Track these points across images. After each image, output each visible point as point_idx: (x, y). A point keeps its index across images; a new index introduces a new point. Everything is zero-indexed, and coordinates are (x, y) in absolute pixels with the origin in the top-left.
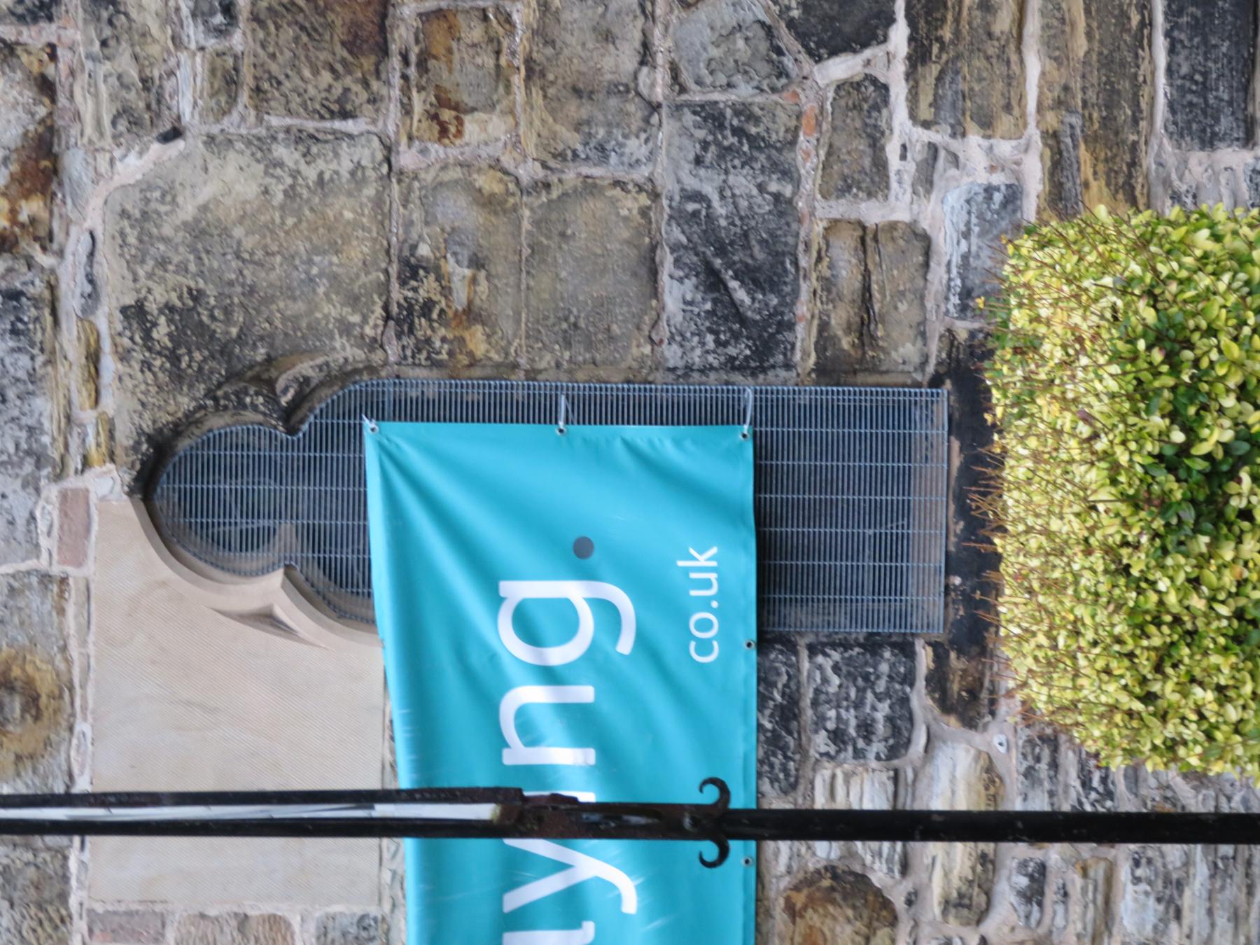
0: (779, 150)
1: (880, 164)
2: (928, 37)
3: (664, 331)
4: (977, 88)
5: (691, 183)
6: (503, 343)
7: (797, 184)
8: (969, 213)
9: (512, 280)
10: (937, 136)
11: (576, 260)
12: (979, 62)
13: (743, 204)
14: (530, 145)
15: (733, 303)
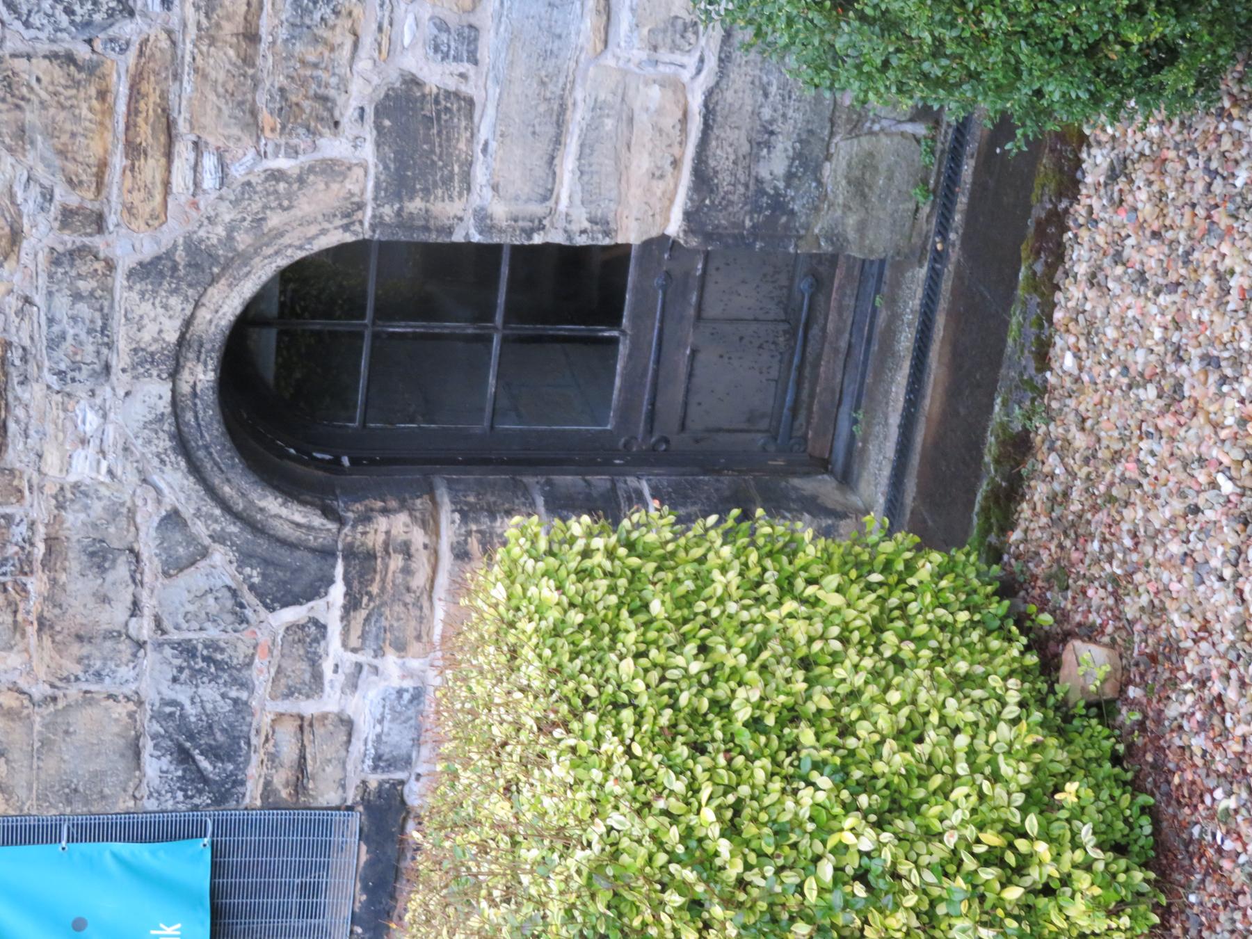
0: (239, 670)
1: (317, 677)
2: (360, 592)
3: (144, 791)
4: (396, 624)
5: (169, 694)
6: (19, 804)
7: (252, 691)
8: (384, 707)
9: (26, 763)
10: (364, 658)
11: (76, 748)
12: (398, 608)
13: (209, 706)
14: (42, 672)
15: (199, 770)
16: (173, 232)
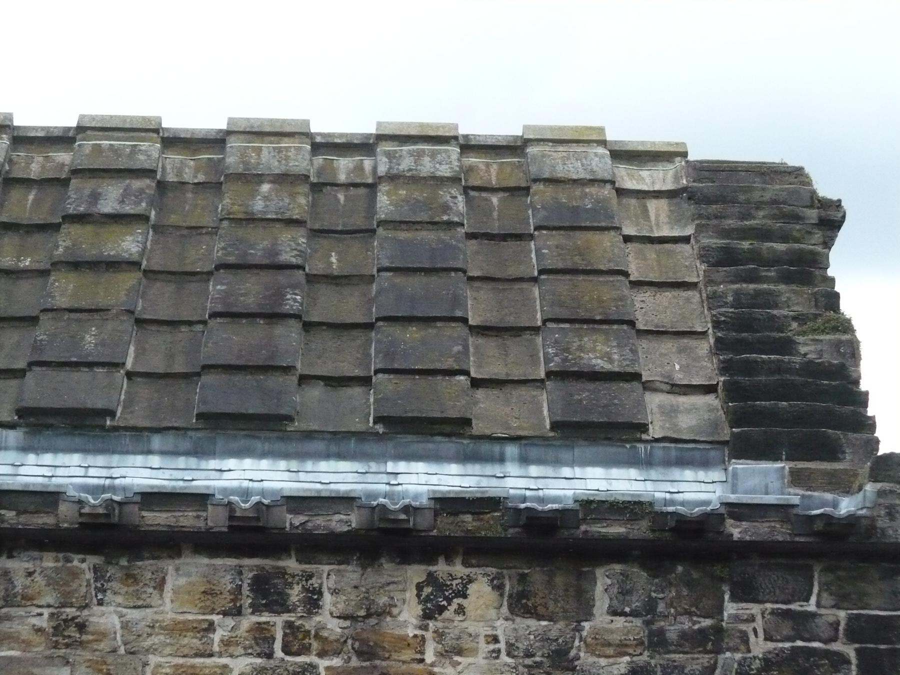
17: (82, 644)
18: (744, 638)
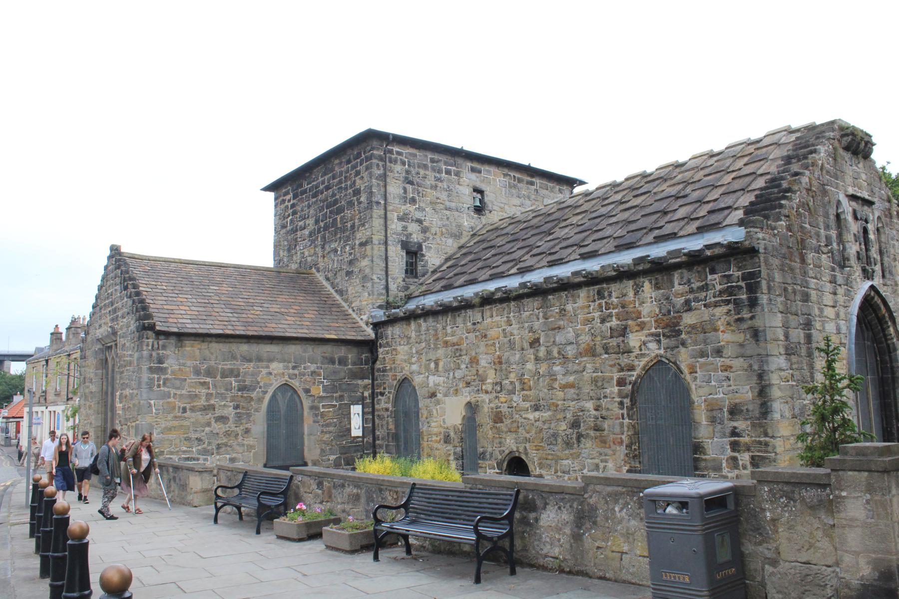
16: (529, 451)
17: (564, 315)
18: (714, 286)
